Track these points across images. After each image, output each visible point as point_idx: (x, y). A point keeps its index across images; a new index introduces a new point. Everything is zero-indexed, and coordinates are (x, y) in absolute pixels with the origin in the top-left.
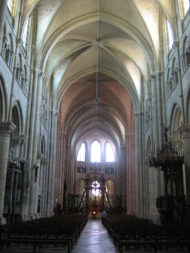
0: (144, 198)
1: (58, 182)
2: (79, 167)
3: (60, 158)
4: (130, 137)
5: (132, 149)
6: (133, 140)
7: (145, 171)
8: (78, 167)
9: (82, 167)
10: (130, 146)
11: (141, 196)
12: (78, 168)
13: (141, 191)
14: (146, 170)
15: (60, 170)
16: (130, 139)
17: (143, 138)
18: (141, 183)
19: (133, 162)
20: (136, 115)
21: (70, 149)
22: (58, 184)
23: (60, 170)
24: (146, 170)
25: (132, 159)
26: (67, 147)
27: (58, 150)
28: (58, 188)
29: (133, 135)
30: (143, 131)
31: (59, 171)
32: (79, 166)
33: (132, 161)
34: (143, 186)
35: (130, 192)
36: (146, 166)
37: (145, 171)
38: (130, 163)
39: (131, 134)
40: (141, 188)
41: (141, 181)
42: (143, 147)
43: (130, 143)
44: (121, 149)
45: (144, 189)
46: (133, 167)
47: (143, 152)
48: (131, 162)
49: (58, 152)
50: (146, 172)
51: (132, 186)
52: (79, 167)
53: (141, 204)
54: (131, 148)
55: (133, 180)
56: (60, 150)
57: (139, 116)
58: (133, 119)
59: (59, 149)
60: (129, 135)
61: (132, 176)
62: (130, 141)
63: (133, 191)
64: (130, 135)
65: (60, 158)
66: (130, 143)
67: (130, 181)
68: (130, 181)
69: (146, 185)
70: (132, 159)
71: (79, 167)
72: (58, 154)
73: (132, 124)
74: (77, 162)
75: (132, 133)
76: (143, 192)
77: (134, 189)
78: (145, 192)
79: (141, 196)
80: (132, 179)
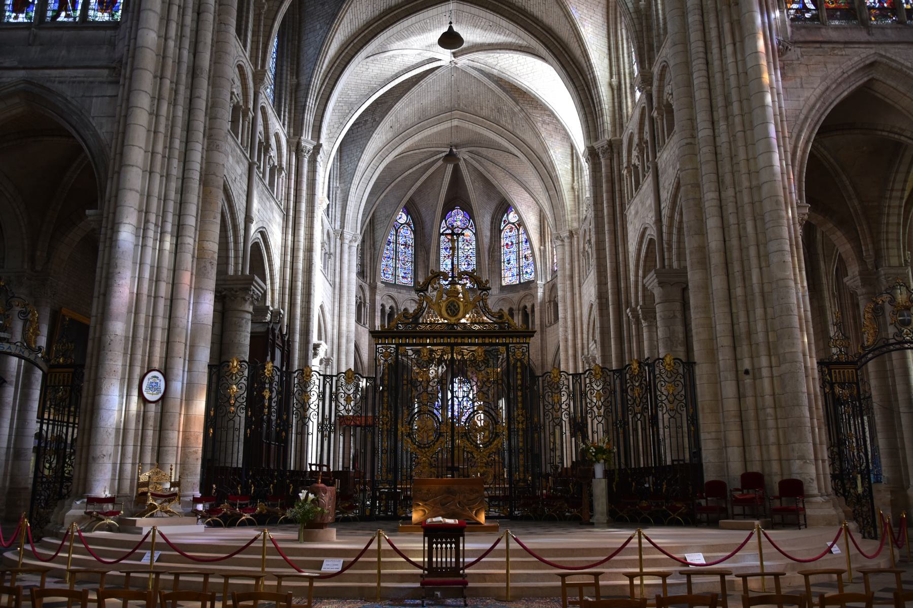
1: (166, 274)
2: (387, 308)
3: (190, 110)
8: (383, 305)
9: (402, 308)
12: (383, 311)
15: (183, 191)
21: (313, 161)
22: (164, 289)
23: (183, 191)
25: (720, 101)
26: (298, 144)
27: (171, 44)
28: (161, 322)
31: (172, 195)
32: (391, 303)
35: (724, 341)
38: (703, 132)
44: (593, 154)
49: (170, 62)
51: (739, 292)
52: (387, 308)
54: (704, 31)
56: (195, 52)
59: (186, 43)
61: (732, 220)
63: (750, 334)
65: (190, 110)
67: (716, 259)
70: (720, 101)
71: (391, 308)
72: (168, 73)
74: (380, 285)
77: (759, 311)
80: (734, 242)
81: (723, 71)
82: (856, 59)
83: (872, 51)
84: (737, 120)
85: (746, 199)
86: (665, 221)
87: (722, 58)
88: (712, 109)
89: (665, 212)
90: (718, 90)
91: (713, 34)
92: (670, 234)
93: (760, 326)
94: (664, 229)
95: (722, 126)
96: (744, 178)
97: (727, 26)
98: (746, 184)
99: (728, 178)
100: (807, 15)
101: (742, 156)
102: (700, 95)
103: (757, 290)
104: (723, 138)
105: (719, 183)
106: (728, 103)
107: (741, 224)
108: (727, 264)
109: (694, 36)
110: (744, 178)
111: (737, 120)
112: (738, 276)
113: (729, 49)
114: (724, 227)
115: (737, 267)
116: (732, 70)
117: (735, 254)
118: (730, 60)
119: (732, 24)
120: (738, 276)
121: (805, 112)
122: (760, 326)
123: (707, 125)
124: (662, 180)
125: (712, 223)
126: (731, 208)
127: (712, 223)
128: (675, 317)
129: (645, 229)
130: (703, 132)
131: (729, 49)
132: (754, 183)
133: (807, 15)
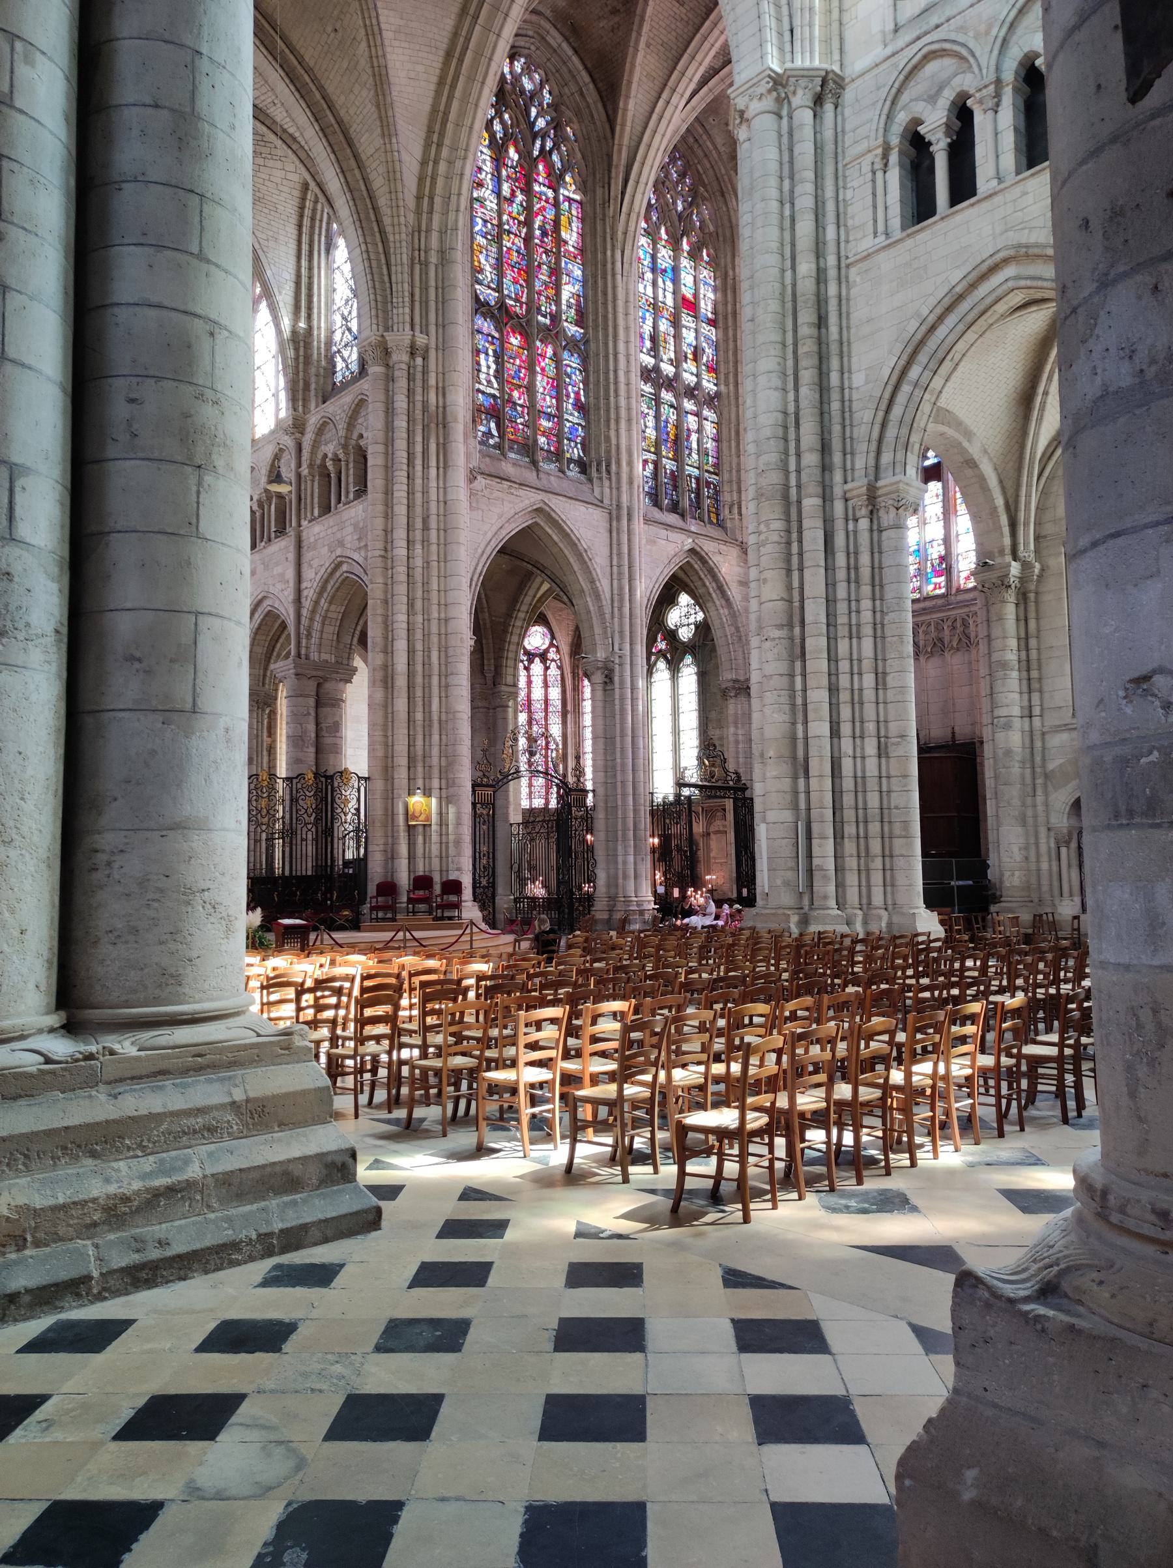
0: (848, 784)
4: (400, 357)
5: (419, 448)
6: (432, 381)
7: (853, 568)
10: (401, 423)
11: (820, 766)
13: (820, 728)
14: (865, 559)
16: (401, 375)
17: (832, 289)
18: (818, 664)
19: (425, 542)
20: (778, 82)
24: (865, 559)
25: (419, 524)
29: (433, 345)
30: (831, 233)
33: (418, 535)
34: (833, 690)
35: (403, 761)
36: (864, 524)
37: (853, 568)
38: (401, 551)
39: (421, 340)
40: (819, 696)
41: (816, 644)
42: (835, 363)
43: (401, 402)
45: (845, 712)
46: (426, 583)
47: (835, 406)
48: (410, 542)
50: (865, 572)
51: (419, 716)
53: (824, 827)
54: (410, 442)
55: (427, 676)
57: (801, 98)
58: (435, 225)
60: (400, 338)
61: (419, 646)
62: (402, 384)
64: (407, 342)
66: (401, 402)
67: (401, 682)
68: (401, 682)
69: (869, 680)
73: (425, 264)
75: (425, 331)
76: (835, 733)
78: (858, 737)
79: (820, 766)
80: (419, 668)
81: (425, 492)
82: (527, 502)
83: (540, 497)
84: (434, 548)
85: (434, 630)
86: (307, 604)
87: (425, 478)
88: (409, 528)
89: (309, 593)
90: (418, 510)
91: (419, 448)
92: (312, 620)
93: (435, 751)
94: (304, 612)
95: (418, 549)
96: (435, 608)
97: (433, 447)
98: (435, 615)
99: (419, 604)
100: (491, 442)
101: (434, 586)
102: (401, 510)
103: (435, 717)
104: (418, 562)
105: (411, 604)
106: (426, 528)
107: (427, 651)
108: (410, 687)
109: (401, 444)
110: (435, 608)
111: (434, 548)
112: (419, 701)
113: (433, 472)
114: (411, 651)
115: (419, 693)
116: (433, 495)
117: (419, 680)
118: (433, 484)
119: (438, 445)
120: (419, 701)
121: (482, 546)
122: (435, 751)
123: (404, 544)
124: (307, 556)
125: (401, 645)
126: (419, 635)
127: (401, 645)
128: (309, 714)
129: (265, 597)
130: (401, 551)
131: (433, 472)
132: (443, 615)
133: (491, 442)
